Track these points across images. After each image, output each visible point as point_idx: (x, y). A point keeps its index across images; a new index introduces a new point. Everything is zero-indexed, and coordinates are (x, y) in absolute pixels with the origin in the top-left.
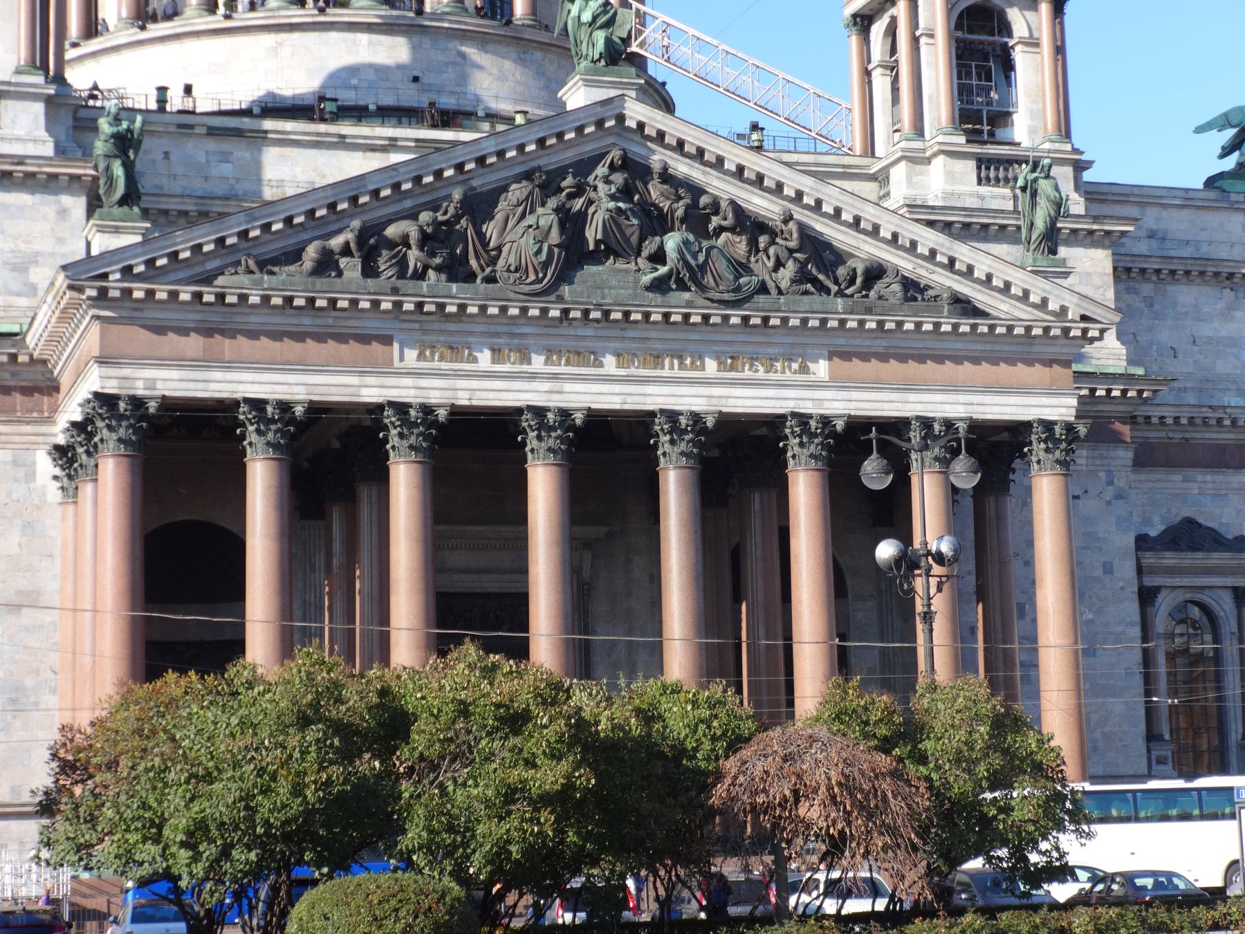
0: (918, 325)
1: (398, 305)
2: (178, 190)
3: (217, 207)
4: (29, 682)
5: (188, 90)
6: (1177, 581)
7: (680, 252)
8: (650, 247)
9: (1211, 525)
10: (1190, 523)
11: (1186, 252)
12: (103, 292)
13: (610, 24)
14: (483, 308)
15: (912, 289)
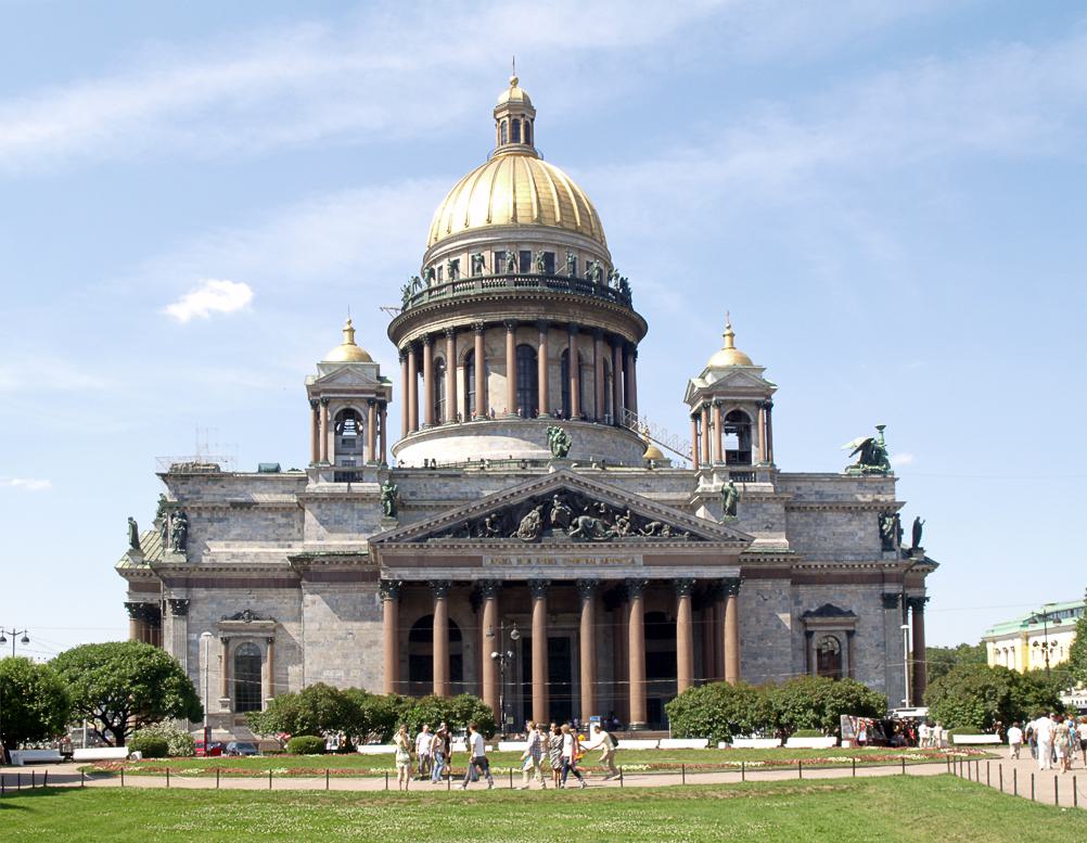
0: (675, 545)
1: (482, 546)
2: (429, 497)
3: (443, 503)
4: (375, 671)
5: (434, 461)
6: (821, 629)
7: (585, 522)
8: (574, 522)
9: (838, 606)
10: (829, 606)
11: (832, 499)
12: (382, 547)
13: (563, 442)
14: (513, 546)
15: (675, 530)
